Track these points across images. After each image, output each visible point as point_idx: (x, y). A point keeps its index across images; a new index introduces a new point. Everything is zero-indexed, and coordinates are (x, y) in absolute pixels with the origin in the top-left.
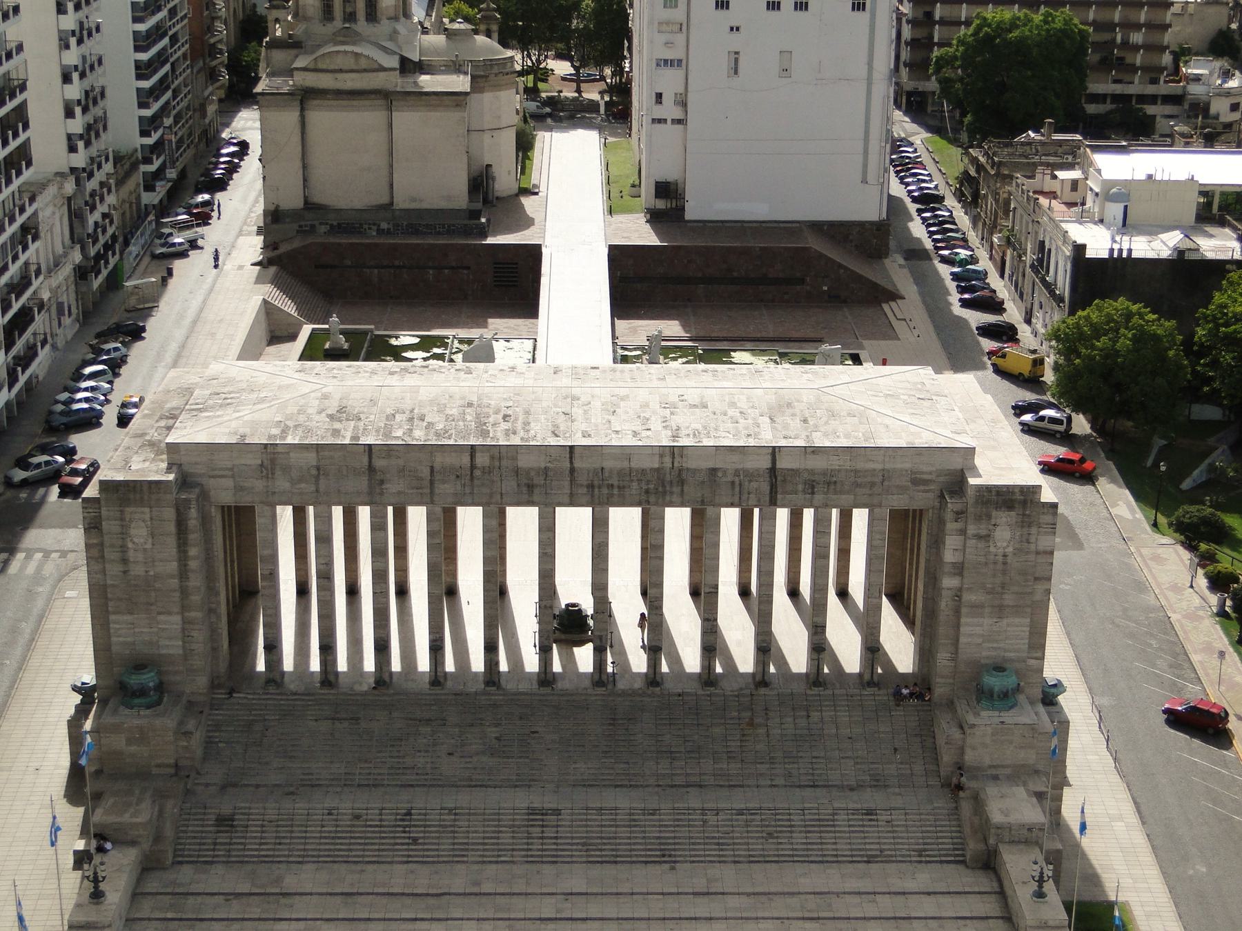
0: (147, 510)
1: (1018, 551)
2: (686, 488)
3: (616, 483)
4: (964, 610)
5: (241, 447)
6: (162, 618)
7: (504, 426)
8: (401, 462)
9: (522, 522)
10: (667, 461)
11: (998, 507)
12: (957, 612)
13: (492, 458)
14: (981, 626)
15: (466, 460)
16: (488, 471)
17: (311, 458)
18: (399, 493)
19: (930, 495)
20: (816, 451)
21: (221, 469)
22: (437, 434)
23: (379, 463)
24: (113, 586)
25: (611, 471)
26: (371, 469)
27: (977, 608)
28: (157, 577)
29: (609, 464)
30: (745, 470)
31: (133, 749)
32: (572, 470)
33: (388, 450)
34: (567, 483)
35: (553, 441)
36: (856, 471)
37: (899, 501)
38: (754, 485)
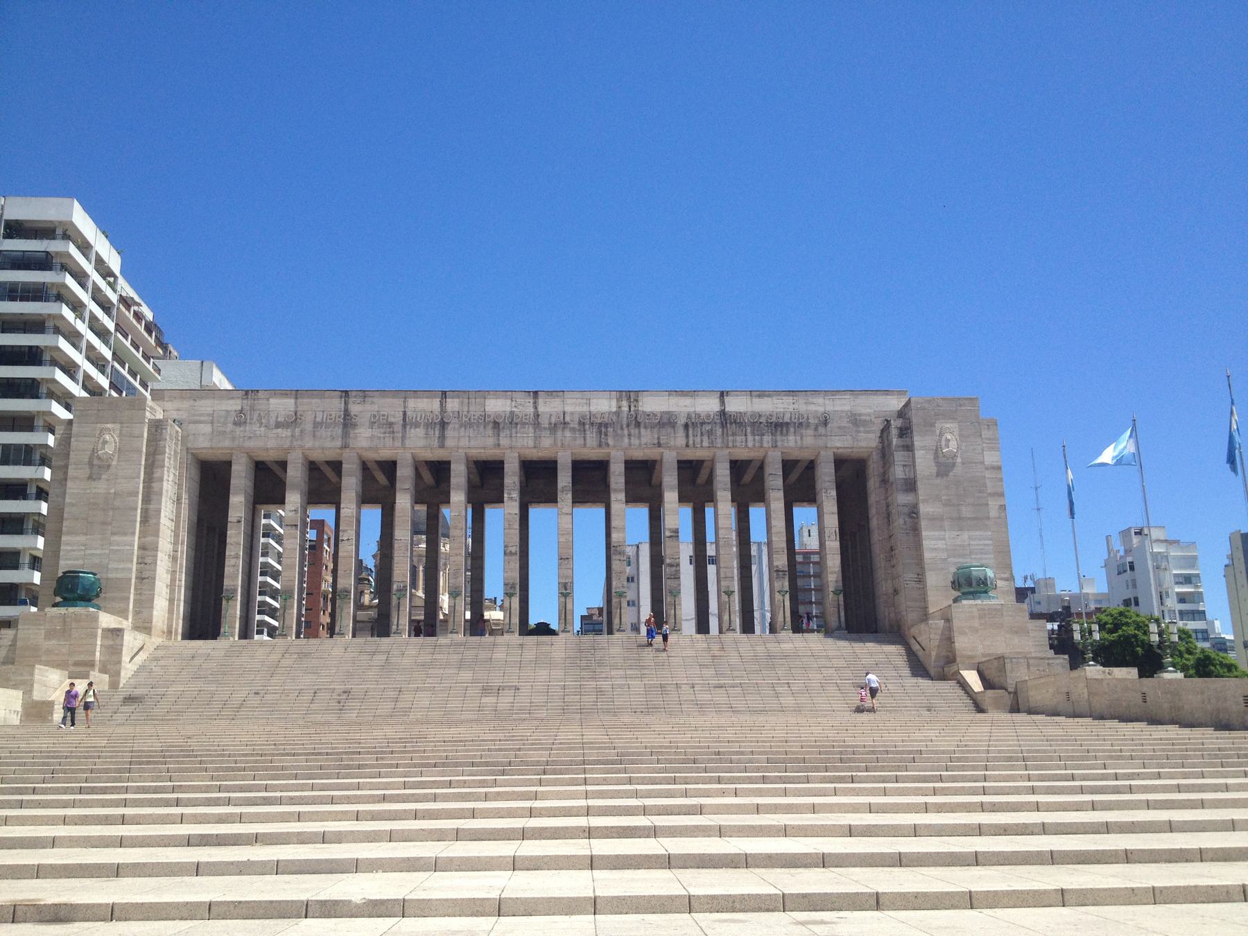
0: (118, 426)
2: (643, 430)
8: (375, 408)
12: (915, 530)
14: (944, 539)
18: (372, 438)
19: (871, 436)
21: (202, 415)
23: (355, 408)
24: (73, 505)
25: (572, 413)
26: (347, 413)
27: (936, 520)
29: (568, 409)
32: (537, 415)
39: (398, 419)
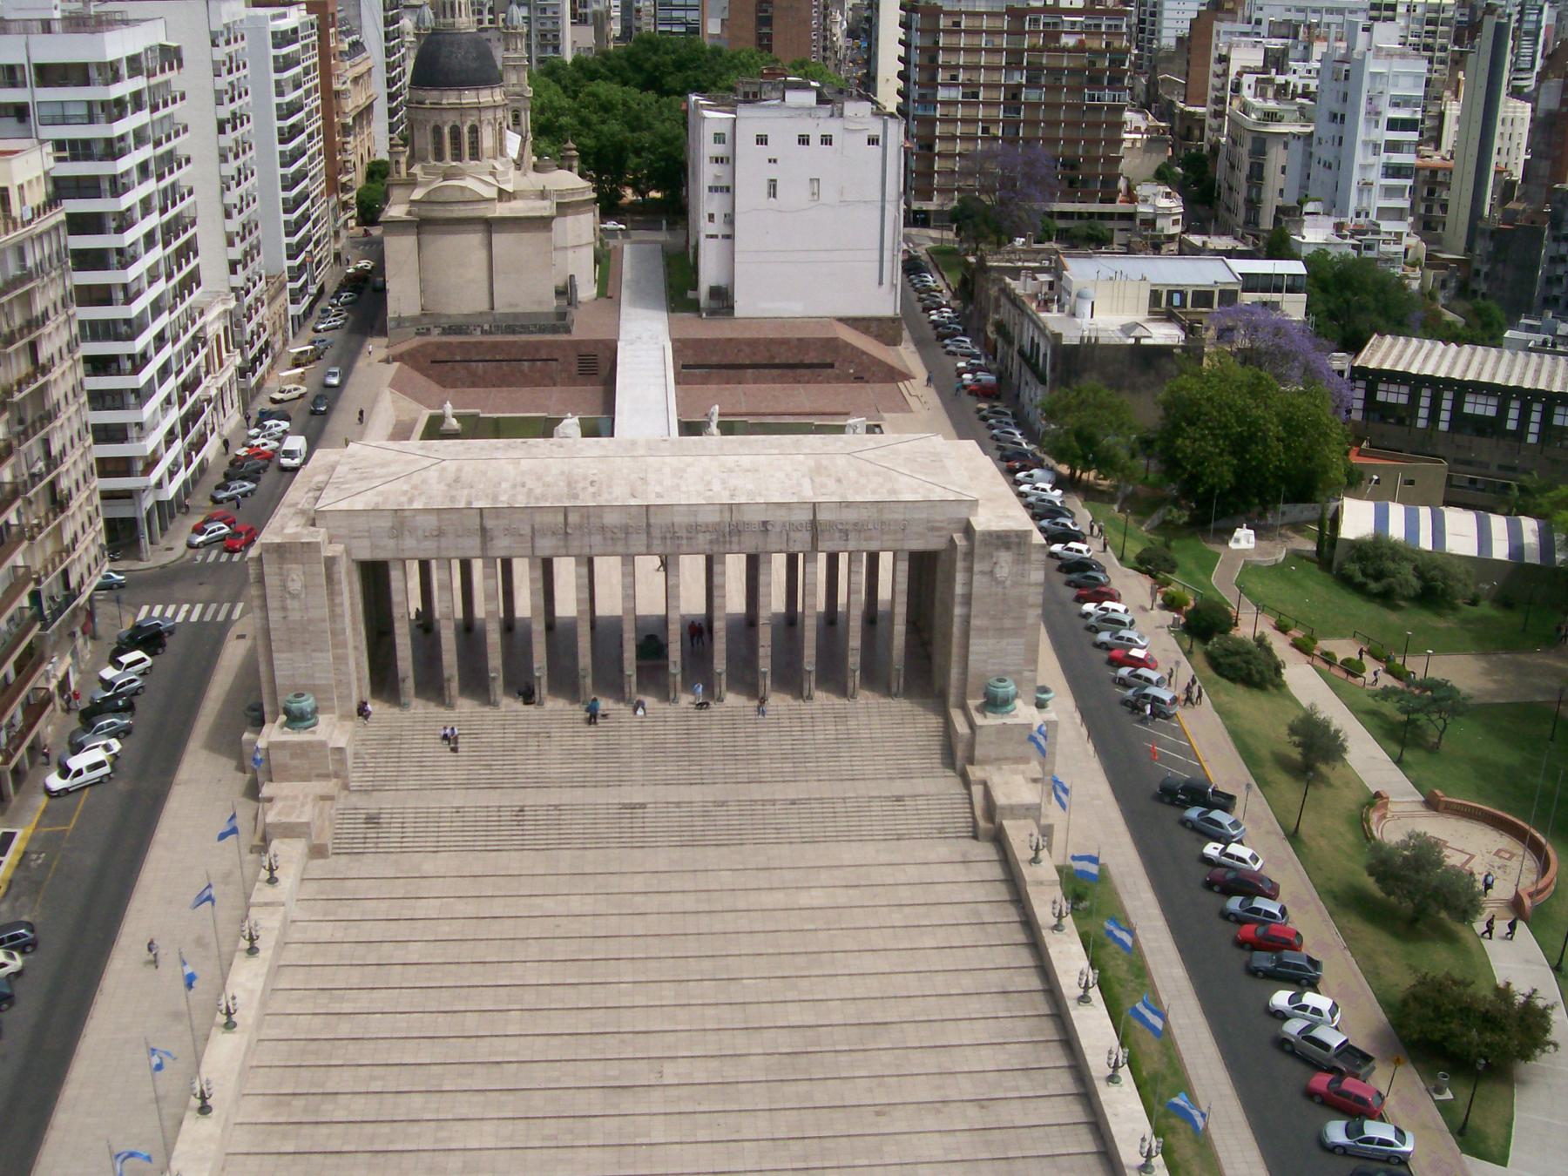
1: (1015, 584)
3: (684, 534)
4: (972, 633)
5: (375, 512)
6: (315, 655)
7: (591, 490)
9: (608, 569)
10: (727, 515)
11: (997, 548)
13: (582, 516)
15: (561, 518)
16: (580, 527)
17: (432, 522)
20: (849, 504)
22: (537, 499)
23: (489, 523)
26: (483, 530)
27: (983, 631)
28: (310, 621)
29: (678, 519)
30: (791, 524)
31: (296, 762)
32: (648, 525)
33: (497, 511)
34: (644, 536)
35: (633, 502)
36: (883, 523)
37: (918, 545)
38: (799, 535)
39: (527, 530)
